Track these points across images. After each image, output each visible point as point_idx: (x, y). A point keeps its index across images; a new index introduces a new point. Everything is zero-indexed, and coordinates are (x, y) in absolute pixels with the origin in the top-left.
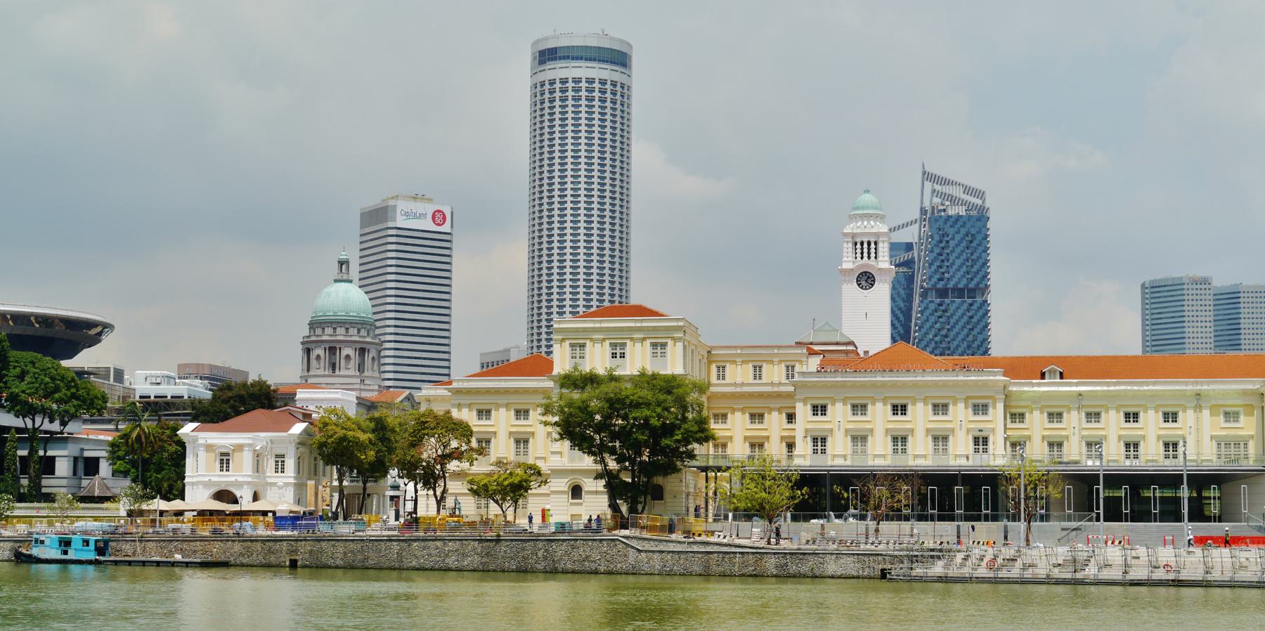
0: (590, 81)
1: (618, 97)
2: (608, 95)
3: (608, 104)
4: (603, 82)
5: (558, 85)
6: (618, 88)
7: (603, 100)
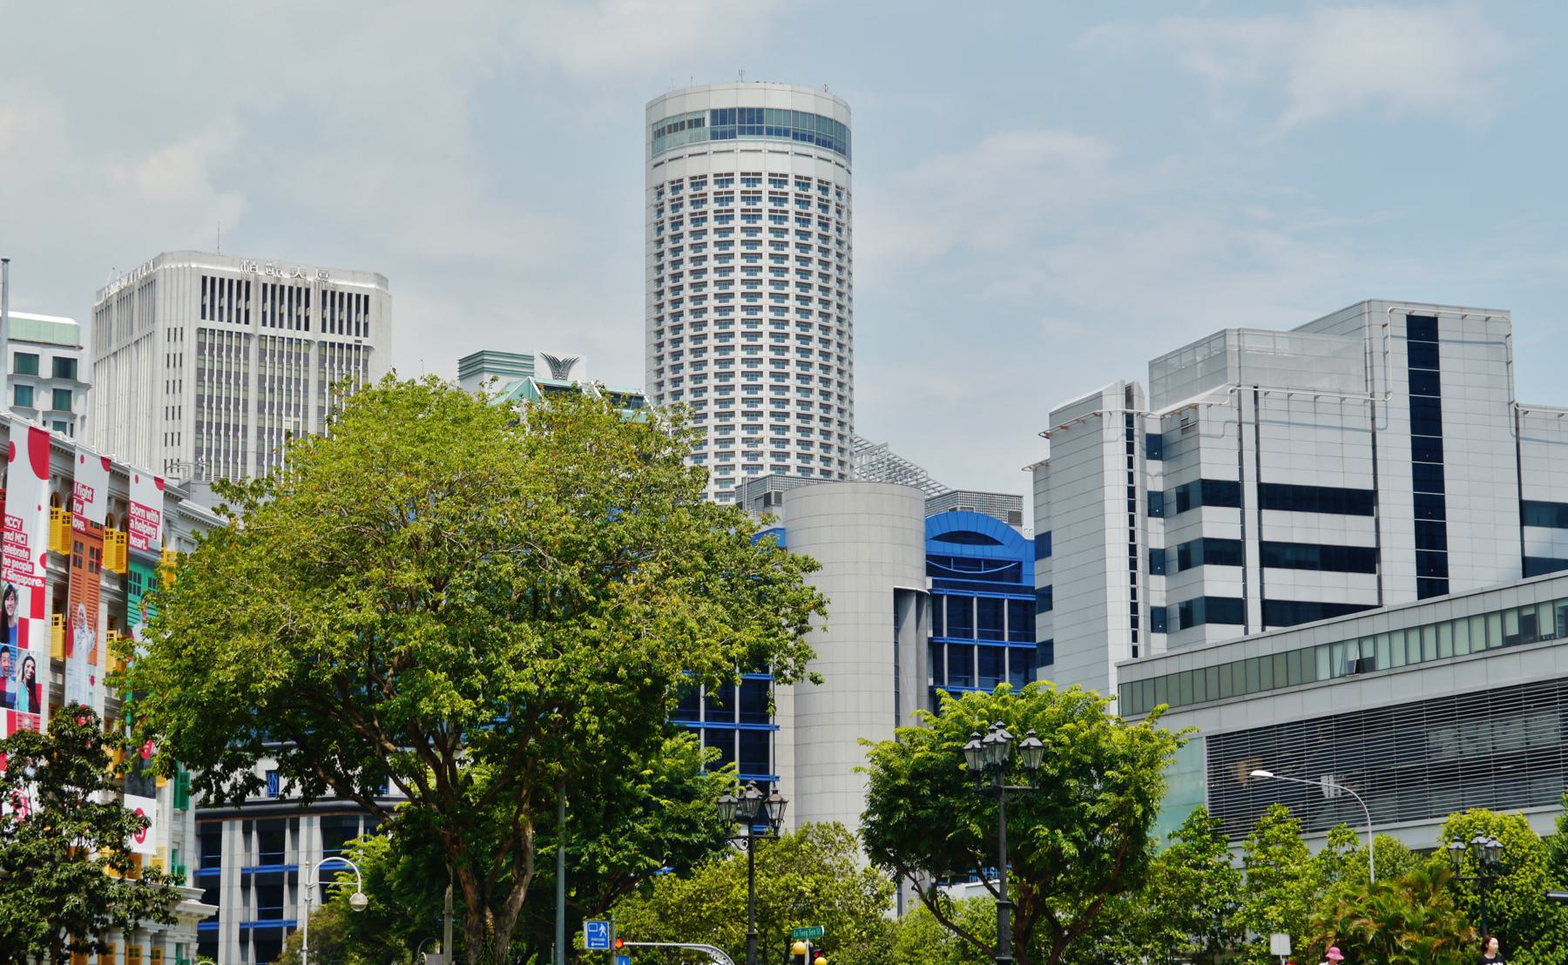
0: (779, 180)
1: (832, 213)
2: (814, 210)
3: (814, 227)
4: (803, 182)
5: (711, 188)
6: (832, 195)
7: (803, 220)
